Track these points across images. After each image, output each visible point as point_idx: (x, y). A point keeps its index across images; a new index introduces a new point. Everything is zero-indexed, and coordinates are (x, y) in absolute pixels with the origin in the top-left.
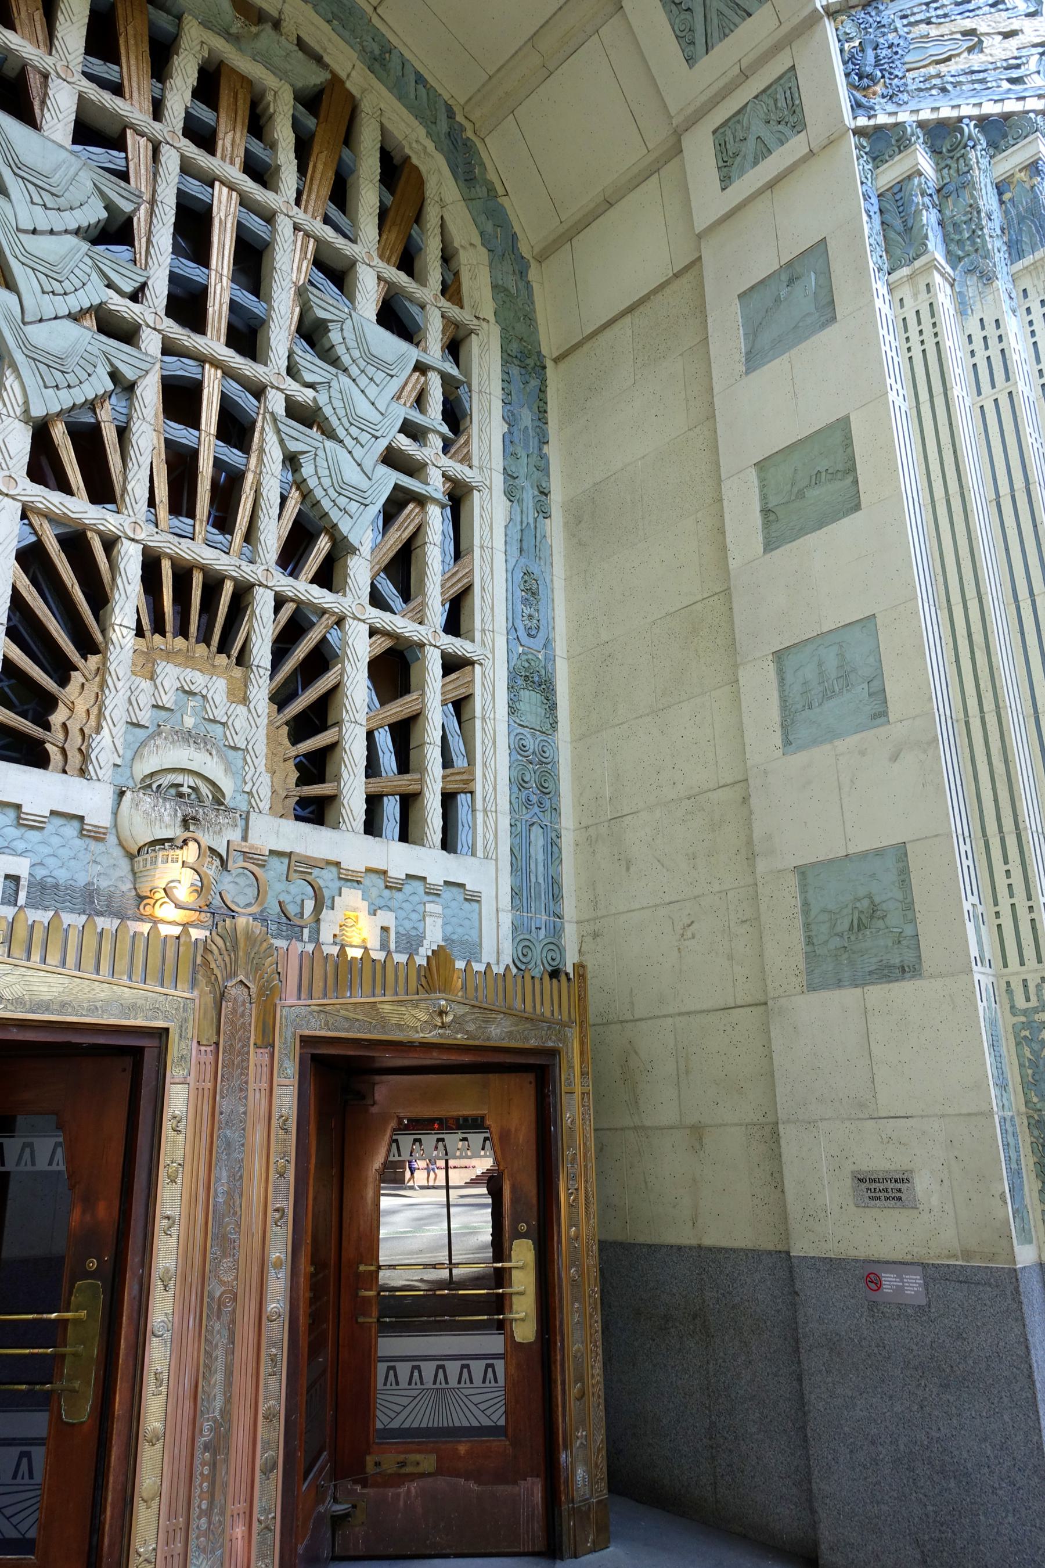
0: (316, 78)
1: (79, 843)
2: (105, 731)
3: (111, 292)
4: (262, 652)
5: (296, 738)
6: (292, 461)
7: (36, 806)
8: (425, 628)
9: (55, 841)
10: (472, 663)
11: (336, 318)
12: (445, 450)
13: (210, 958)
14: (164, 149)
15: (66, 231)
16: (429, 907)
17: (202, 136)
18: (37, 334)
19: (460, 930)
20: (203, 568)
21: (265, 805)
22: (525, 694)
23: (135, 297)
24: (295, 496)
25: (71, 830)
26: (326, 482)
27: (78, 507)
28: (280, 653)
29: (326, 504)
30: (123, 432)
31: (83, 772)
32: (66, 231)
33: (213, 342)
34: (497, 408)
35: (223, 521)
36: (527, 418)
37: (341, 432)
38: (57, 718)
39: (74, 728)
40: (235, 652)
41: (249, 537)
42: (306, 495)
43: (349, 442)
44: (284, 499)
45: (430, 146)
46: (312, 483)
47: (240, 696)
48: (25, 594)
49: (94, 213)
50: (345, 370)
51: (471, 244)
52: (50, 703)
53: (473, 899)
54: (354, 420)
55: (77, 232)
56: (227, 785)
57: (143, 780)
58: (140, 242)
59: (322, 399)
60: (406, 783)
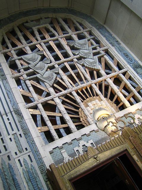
0: (49, 20)
1: (96, 133)
2: (88, 117)
3: (48, 64)
4: (99, 92)
5: (112, 100)
6: (83, 66)
7: (87, 133)
8: (117, 72)
9: (93, 135)
10: (127, 71)
13: (124, 136)
14: (41, 43)
17: (43, 38)
18: (44, 76)
21: (115, 112)
22: (138, 70)
24: (87, 69)
25: (94, 132)
27: (64, 92)
29: (91, 67)
30: (62, 79)
31: (90, 124)
33: (63, 59)
34: (102, 36)
35: (81, 80)
36: (107, 34)
37: (86, 57)
38: (81, 120)
40: (95, 95)
41: (86, 79)
42: (88, 68)
43: (88, 57)
44: (86, 71)
46: (87, 66)
49: (40, 57)
50: (80, 49)
52: (79, 119)
54: (86, 54)
55: (40, 61)
57: (97, 120)
58: (47, 56)
59: (80, 55)
60: (131, 95)
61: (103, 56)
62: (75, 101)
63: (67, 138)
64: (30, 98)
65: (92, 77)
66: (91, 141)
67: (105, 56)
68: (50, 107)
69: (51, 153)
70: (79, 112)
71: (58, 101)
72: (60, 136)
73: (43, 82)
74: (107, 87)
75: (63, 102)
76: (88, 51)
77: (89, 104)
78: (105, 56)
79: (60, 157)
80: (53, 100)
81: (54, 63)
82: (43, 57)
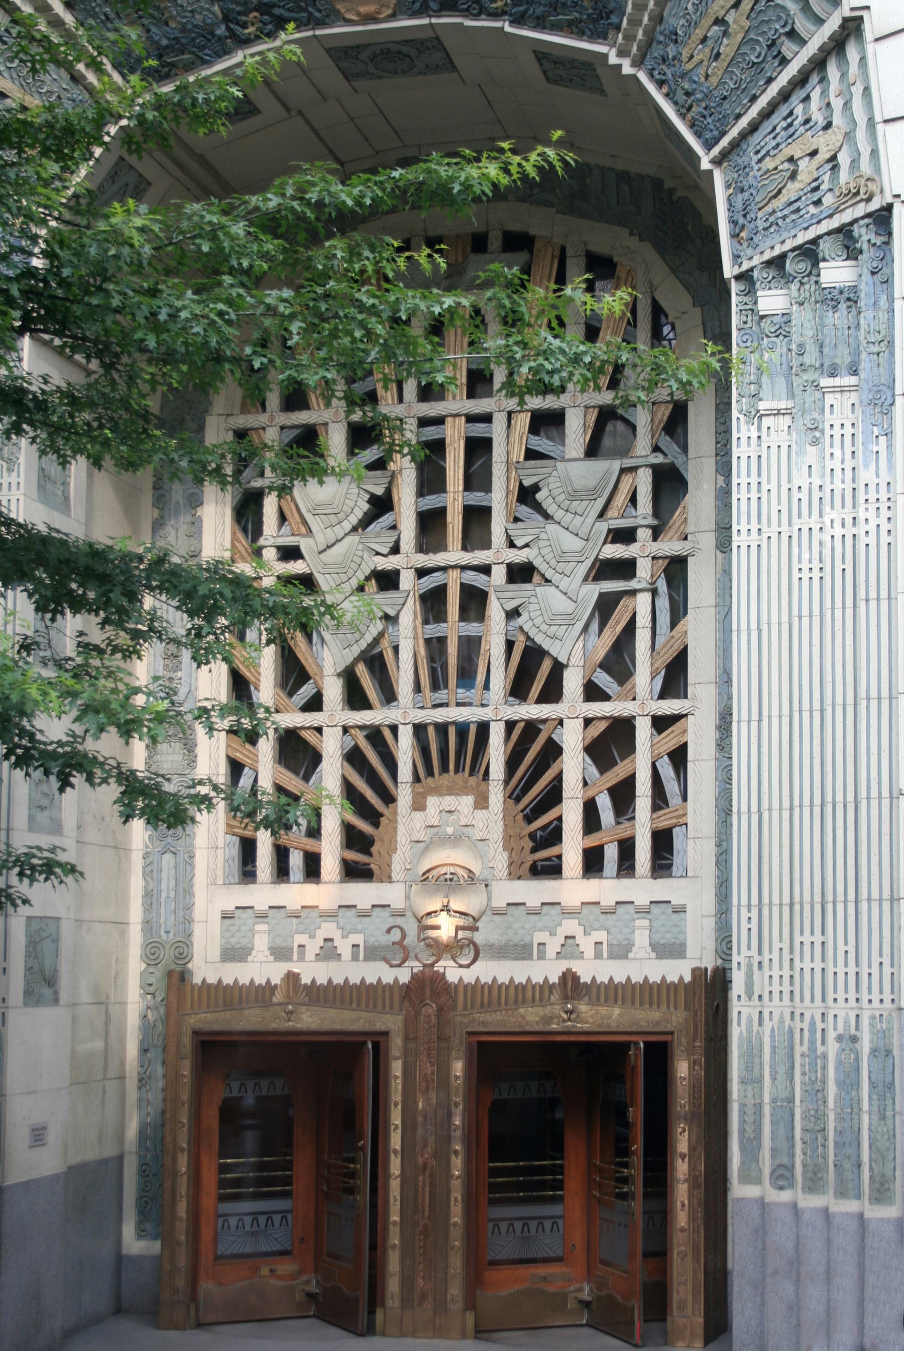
6: (513, 614)
10: (686, 715)
11: (542, 477)
12: (655, 538)
15: (346, 534)
16: (638, 923)
19: (669, 936)
20: (454, 723)
23: (395, 550)
26: (538, 621)
28: (512, 764)
30: (396, 649)
32: (346, 534)
38: (374, 850)
39: (384, 853)
42: (528, 638)
45: (634, 242)
46: (526, 628)
47: (482, 802)
48: (351, 780)
51: (683, 313)
53: (680, 910)
54: (562, 556)
56: (476, 868)
57: (424, 874)
60: (623, 831)
61: (633, 593)
62: (391, 765)
63: (297, 894)
64: (252, 688)
65: (518, 690)
66: (359, 939)
67: (643, 602)
68: (298, 752)
69: (226, 916)
70: (382, 815)
71: (332, 748)
72: (282, 872)
73: (323, 641)
74: (553, 751)
75: (354, 757)
76: (576, 544)
77: (432, 802)
78: (643, 602)
79: (244, 941)
80: (319, 730)
81: (408, 560)
82: (381, 505)
